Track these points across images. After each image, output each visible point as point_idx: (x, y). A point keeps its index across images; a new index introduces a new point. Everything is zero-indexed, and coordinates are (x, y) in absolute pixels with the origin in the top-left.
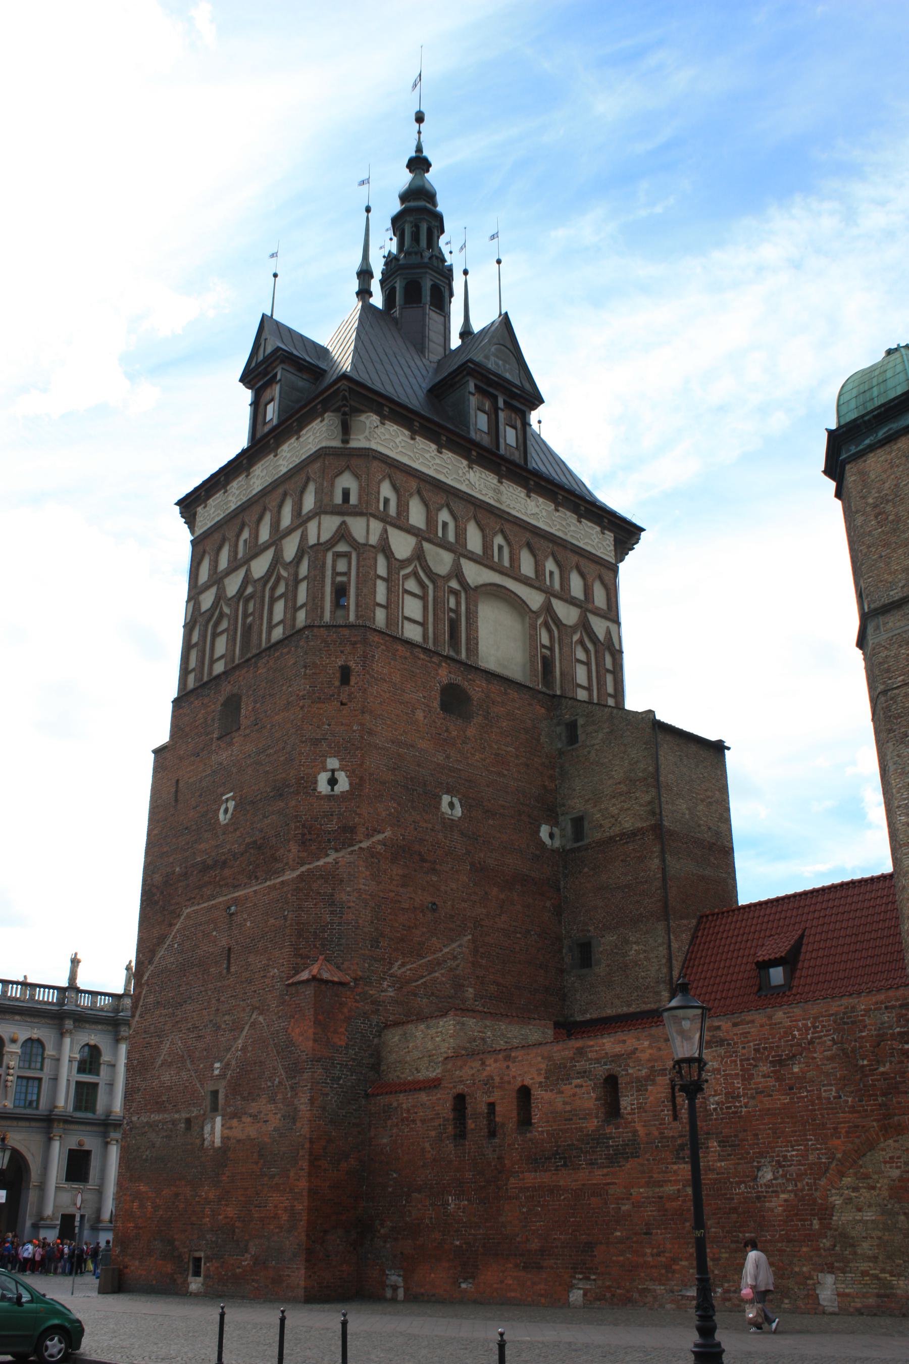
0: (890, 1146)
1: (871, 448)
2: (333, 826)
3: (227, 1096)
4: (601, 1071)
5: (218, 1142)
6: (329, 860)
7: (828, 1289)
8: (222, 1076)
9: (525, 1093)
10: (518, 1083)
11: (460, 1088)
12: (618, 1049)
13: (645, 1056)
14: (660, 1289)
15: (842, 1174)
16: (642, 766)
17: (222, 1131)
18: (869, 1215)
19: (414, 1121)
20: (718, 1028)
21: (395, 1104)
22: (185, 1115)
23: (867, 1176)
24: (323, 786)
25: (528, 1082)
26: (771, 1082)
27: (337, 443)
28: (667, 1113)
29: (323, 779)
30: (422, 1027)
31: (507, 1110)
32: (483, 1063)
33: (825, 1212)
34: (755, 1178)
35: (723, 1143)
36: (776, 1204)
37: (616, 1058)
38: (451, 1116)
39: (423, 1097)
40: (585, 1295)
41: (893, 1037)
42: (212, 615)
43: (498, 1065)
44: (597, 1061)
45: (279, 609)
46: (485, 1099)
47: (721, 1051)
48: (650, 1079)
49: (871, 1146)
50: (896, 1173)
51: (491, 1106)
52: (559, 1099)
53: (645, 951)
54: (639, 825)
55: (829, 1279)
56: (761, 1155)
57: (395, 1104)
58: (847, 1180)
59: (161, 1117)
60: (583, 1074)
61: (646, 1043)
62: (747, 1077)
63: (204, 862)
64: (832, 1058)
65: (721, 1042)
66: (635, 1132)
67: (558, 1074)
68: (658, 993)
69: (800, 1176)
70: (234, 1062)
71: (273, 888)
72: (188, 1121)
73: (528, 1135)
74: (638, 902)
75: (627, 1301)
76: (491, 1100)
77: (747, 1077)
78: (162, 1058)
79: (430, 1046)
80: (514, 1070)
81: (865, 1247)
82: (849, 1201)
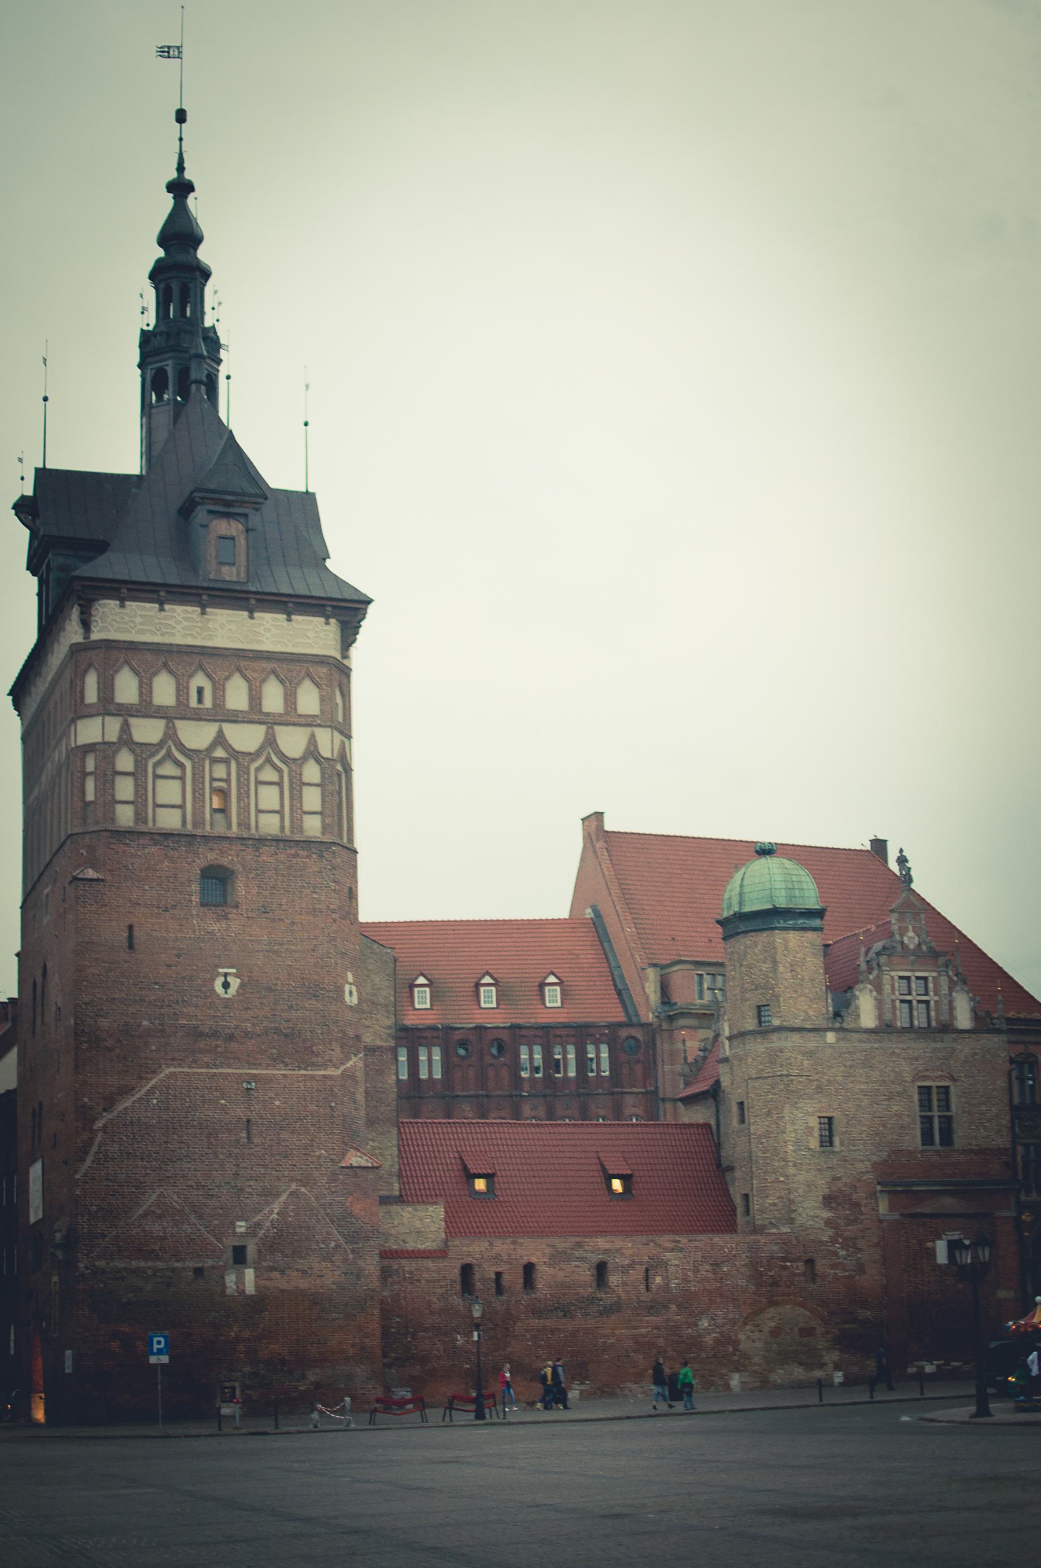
0: (771, 1312)
1: (794, 929)
2: (352, 1034)
3: (260, 1251)
4: (596, 1258)
5: (250, 1288)
6: (351, 1063)
7: (735, 1380)
8: (252, 1232)
9: (529, 1269)
10: (525, 1260)
11: (468, 1260)
12: (608, 1246)
13: (627, 1252)
14: (634, 1386)
15: (746, 1324)
16: (384, 993)
17: (256, 1282)
18: (758, 1344)
19: (418, 1281)
20: (679, 1241)
21: (395, 1267)
22: (192, 1264)
23: (758, 1325)
24: (347, 998)
25: (534, 1260)
26: (710, 1275)
27: (338, 656)
28: (642, 1288)
29: (347, 988)
30: (410, 1209)
31: (513, 1278)
32: (491, 1244)
33: (736, 1343)
34: (697, 1325)
35: (679, 1306)
36: (709, 1340)
37: (607, 1251)
38: (459, 1278)
39: (429, 1264)
40: (581, 1393)
41: (778, 1258)
42: (157, 751)
43: (505, 1246)
44: (593, 1252)
45: (269, 798)
46: (494, 1269)
47: (681, 1255)
48: (632, 1265)
49: (762, 1311)
50: (773, 1324)
51: (499, 1275)
52: (561, 1274)
53: (380, 1148)
54: (379, 1043)
55: (736, 1376)
56: (702, 1313)
57: (395, 1267)
58: (748, 1327)
59: (150, 1264)
60: (581, 1259)
61: (630, 1245)
62: (696, 1271)
63: (196, 1028)
64: (744, 1266)
65: (681, 1250)
66: (619, 1297)
67: (558, 1257)
68: (391, 1184)
69: (723, 1325)
70: (268, 1224)
71: (313, 1077)
72: (199, 1272)
73: (533, 1296)
74: (375, 1107)
75: (612, 1394)
76: (499, 1270)
77: (696, 1271)
78: (145, 1207)
79: (418, 1224)
80: (520, 1252)
81: (756, 1360)
82: (749, 1337)
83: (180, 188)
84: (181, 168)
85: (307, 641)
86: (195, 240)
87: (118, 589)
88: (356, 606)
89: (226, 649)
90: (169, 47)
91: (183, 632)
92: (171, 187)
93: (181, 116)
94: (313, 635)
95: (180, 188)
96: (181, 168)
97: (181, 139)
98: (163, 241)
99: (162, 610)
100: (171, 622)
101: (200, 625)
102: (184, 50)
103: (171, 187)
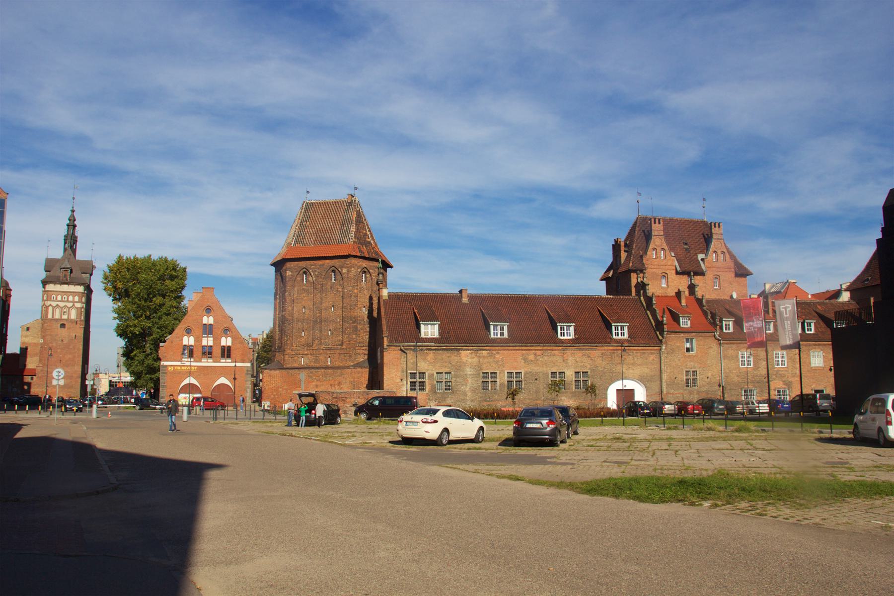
83: (73, 211)
95: (73, 211)
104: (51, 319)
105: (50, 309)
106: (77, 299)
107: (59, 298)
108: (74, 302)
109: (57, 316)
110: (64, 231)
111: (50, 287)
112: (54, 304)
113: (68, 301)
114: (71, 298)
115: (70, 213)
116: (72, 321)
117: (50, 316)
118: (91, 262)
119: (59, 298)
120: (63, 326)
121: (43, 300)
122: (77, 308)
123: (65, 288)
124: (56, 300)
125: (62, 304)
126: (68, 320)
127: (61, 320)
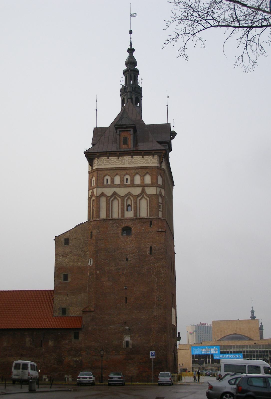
83: (131, 50)
84: (131, 45)
85: (148, 162)
86: (135, 63)
87: (106, 154)
88: (161, 151)
89: (131, 167)
90: (134, 16)
91: (116, 164)
92: (129, 50)
93: (131, 32)
94: (151, 161)
95: (131, 50)
96: (131, 45)
97: (131, 38)
98: (127, 64)
99: (118, 158)
100: (113, 162)
101: (121, 161)
102: (130, 16)
103: (129, 50)
104: (104, 220)
105: (103, 201)
106: (148, 179)
107: (117, 180)
108: (143, 186)
109: (116, 215)
110: (119, 81)
111: (102, 163)
112: (109, 192)
113: (133, 185)
114: (137, 180)
115: (128, 54)
116: (143, 220)
117: (103, 215)
118: (168, 126)
119: (117, 180)
120: (126, 230)
121: (90, 188)
122: (150, 196)
123: (126, 162)
124: (113, 185)
125: (122, 192)
126: (137, 219)
127: (122, 219)
